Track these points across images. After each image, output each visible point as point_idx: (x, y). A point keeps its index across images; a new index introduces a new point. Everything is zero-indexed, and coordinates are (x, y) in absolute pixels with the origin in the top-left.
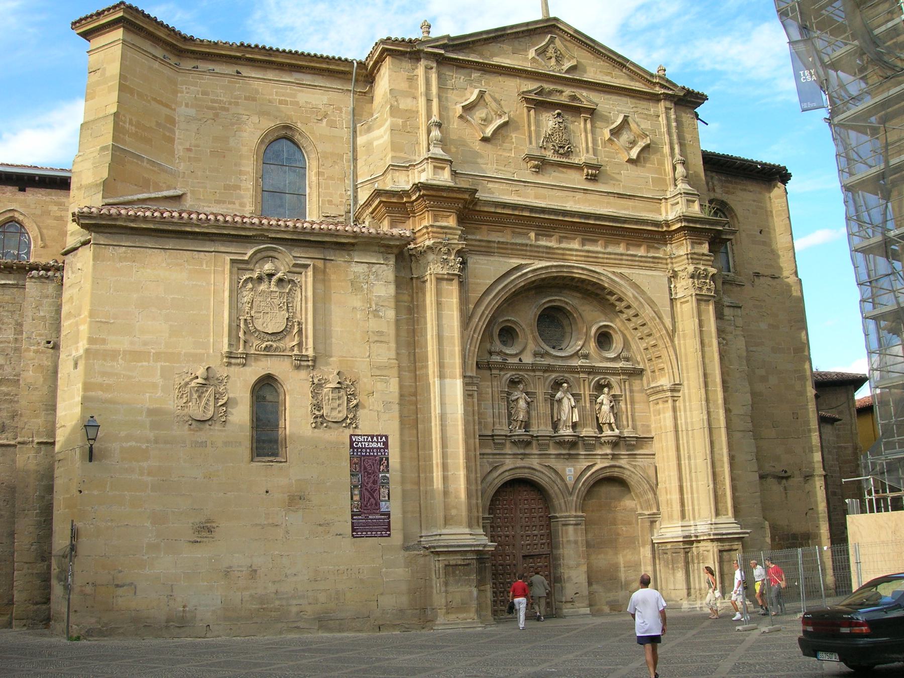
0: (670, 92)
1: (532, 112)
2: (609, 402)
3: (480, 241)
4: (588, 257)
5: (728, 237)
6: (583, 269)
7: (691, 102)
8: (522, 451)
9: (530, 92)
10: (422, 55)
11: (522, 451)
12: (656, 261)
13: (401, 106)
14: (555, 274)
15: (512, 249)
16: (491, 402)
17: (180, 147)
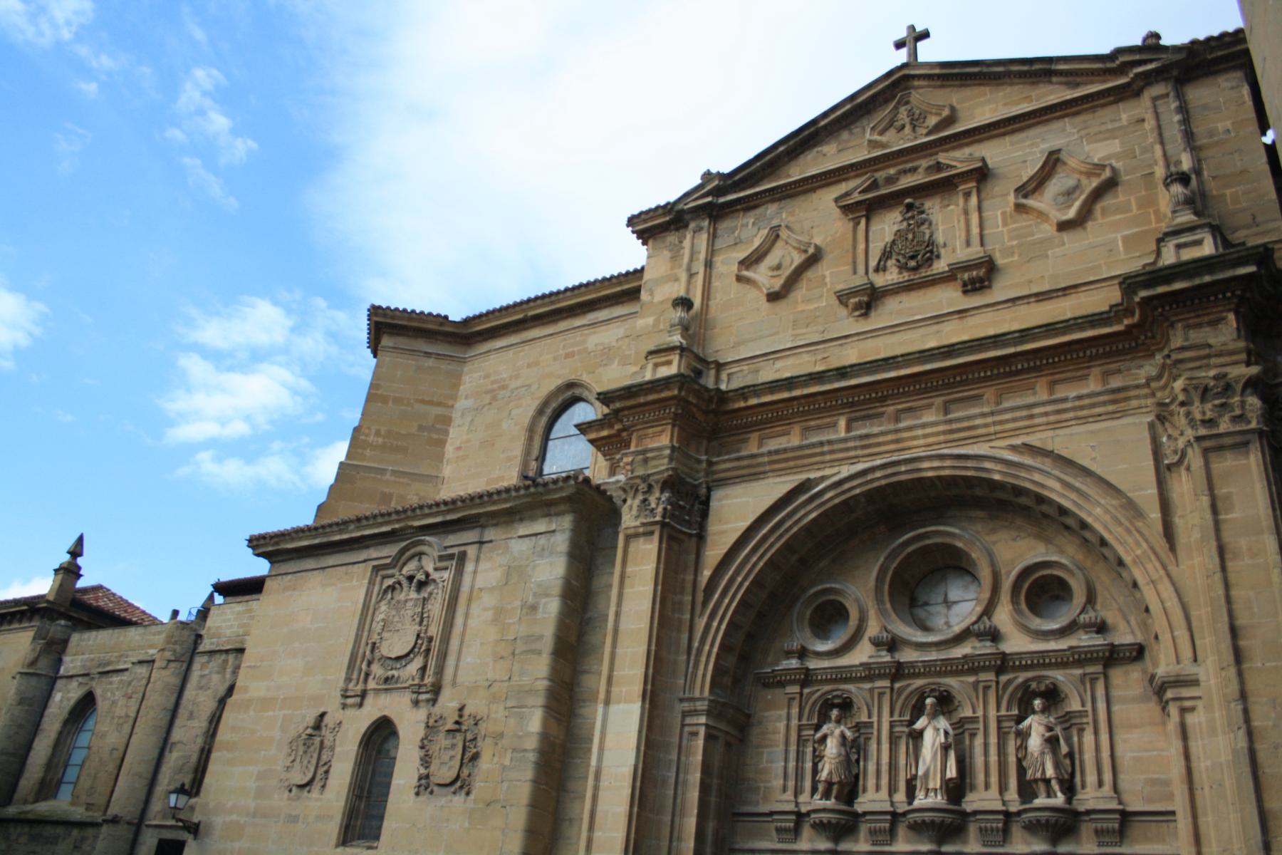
2: (1042, 729)
3: (738, 459)
6: (942, 457)
10: (687, 217)
12: (1122, 395)
14: (883, 482)
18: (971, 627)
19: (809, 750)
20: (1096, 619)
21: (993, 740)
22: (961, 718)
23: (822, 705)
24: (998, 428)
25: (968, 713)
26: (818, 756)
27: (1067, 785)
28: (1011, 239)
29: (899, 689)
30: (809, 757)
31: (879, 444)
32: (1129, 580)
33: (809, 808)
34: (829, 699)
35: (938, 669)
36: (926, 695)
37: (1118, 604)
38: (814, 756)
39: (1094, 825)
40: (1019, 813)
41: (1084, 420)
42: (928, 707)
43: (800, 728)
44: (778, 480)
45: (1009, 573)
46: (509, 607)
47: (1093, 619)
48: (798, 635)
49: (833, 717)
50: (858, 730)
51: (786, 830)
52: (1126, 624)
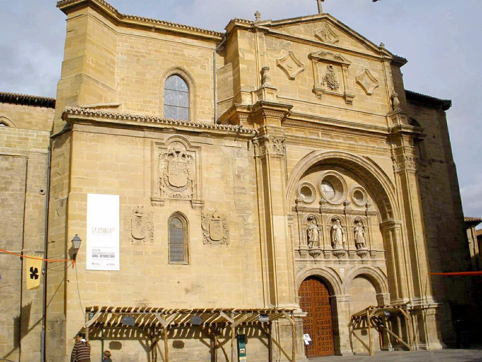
0: (388, 57)
1: (317, 64)
4: (349, 147)
5: (422, 138)
6: (347, 154)
7: (398, 63)
9: (315, 53)
12: (386, 150)
13: (246, 58)
15: (309, 142)
17: (118, 78)
24: (360, 150)
28: (356, 91)
31: (332, 145)
41: (377, 154)
44: (303, 147)
46: (228, 174)
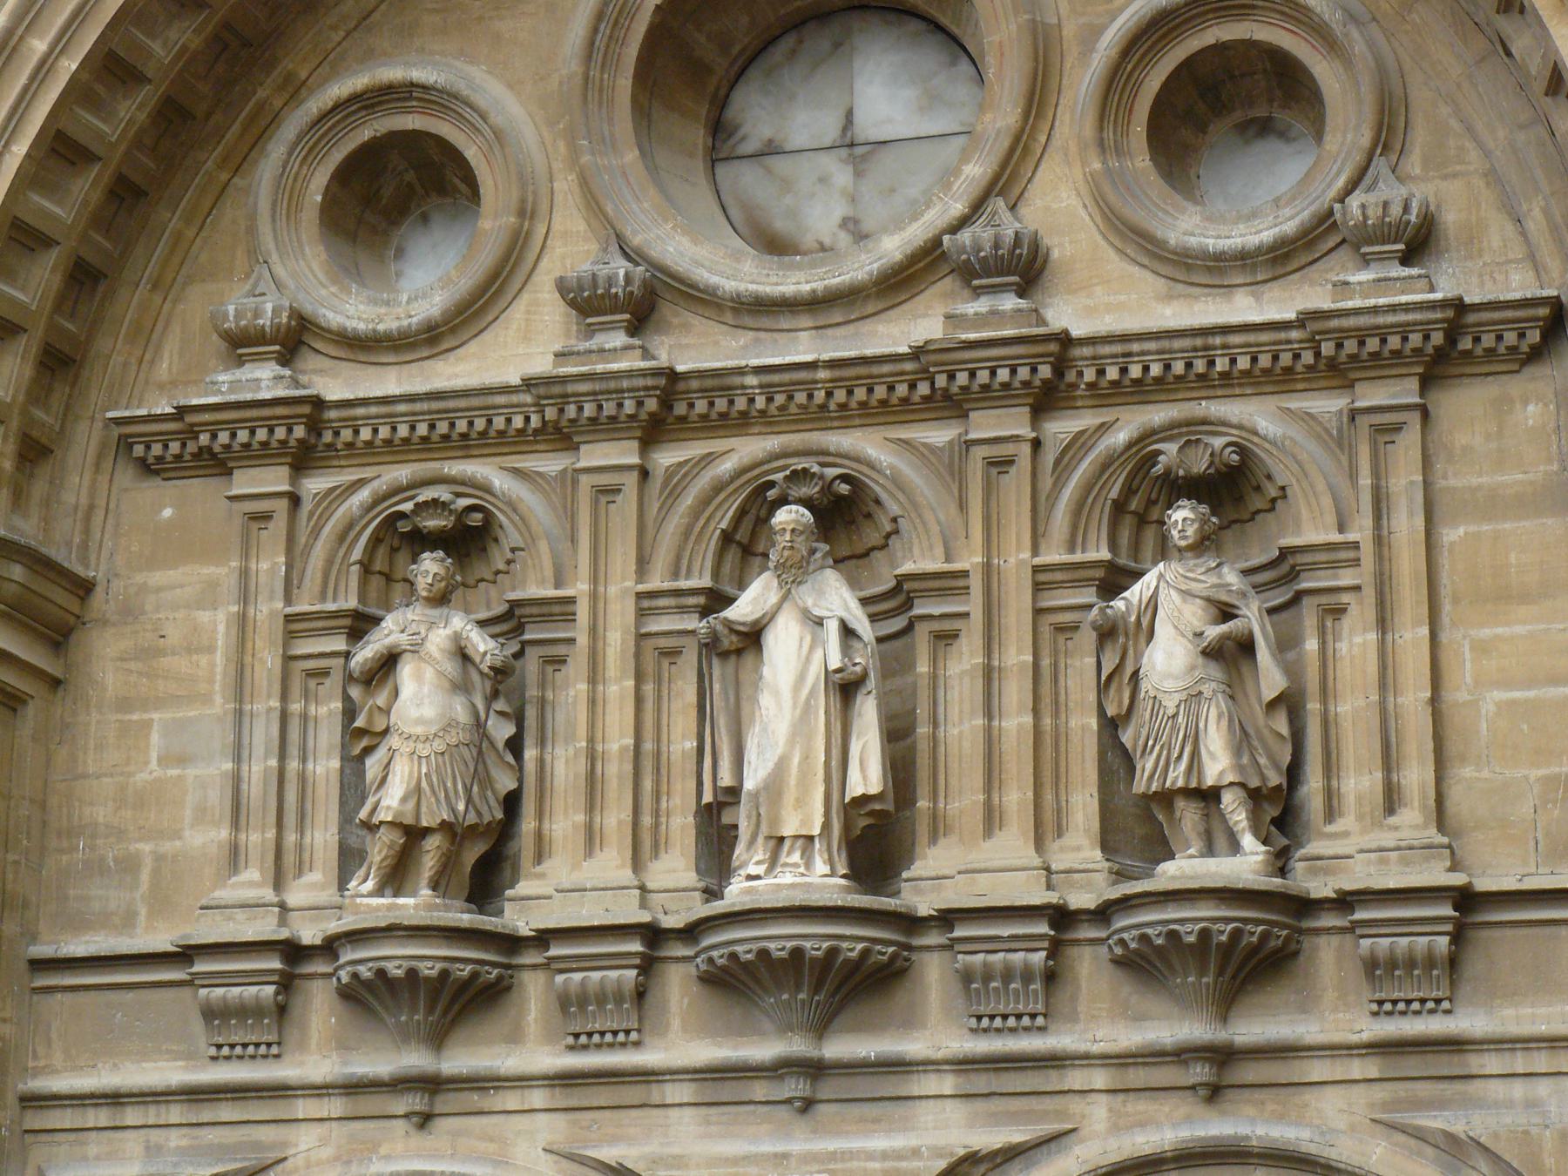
2: (1194, 615)
8: (415, 1060)
11: (415, 1060)
16: (220, 704)
18: (946, 238)
19: (328, 709)
20: (1406, 209)
21: (1016, 655)
22: (902, 580)
23: (376, 541)
25: (920, 560)
26: (362, 732)
27: (1273, 812)
29: (671, 472)
30: (328, 735)
32: (1536, 67)
33: (334, 926)
34: (402, 515)
35: (820, 396)
36: (772, 494)
37: (1487, 154)
38: (352, 733)
39: (1365, 943)
40: (1103, 913)
42: (783, 540)
43: (294, 626)
45: (1096, 32)
47: (1396, 211)
48: (279, 270)
49: (422, 583)
50: (519, 629)
51: (244, 1012)
52: (1510, 228)
